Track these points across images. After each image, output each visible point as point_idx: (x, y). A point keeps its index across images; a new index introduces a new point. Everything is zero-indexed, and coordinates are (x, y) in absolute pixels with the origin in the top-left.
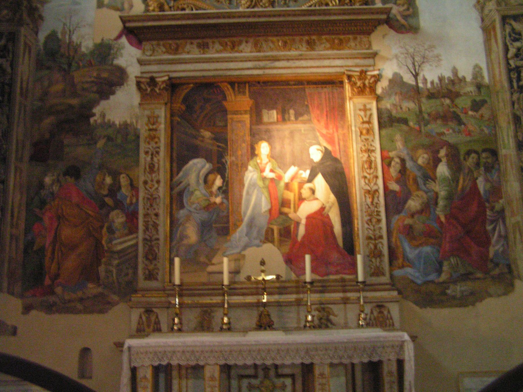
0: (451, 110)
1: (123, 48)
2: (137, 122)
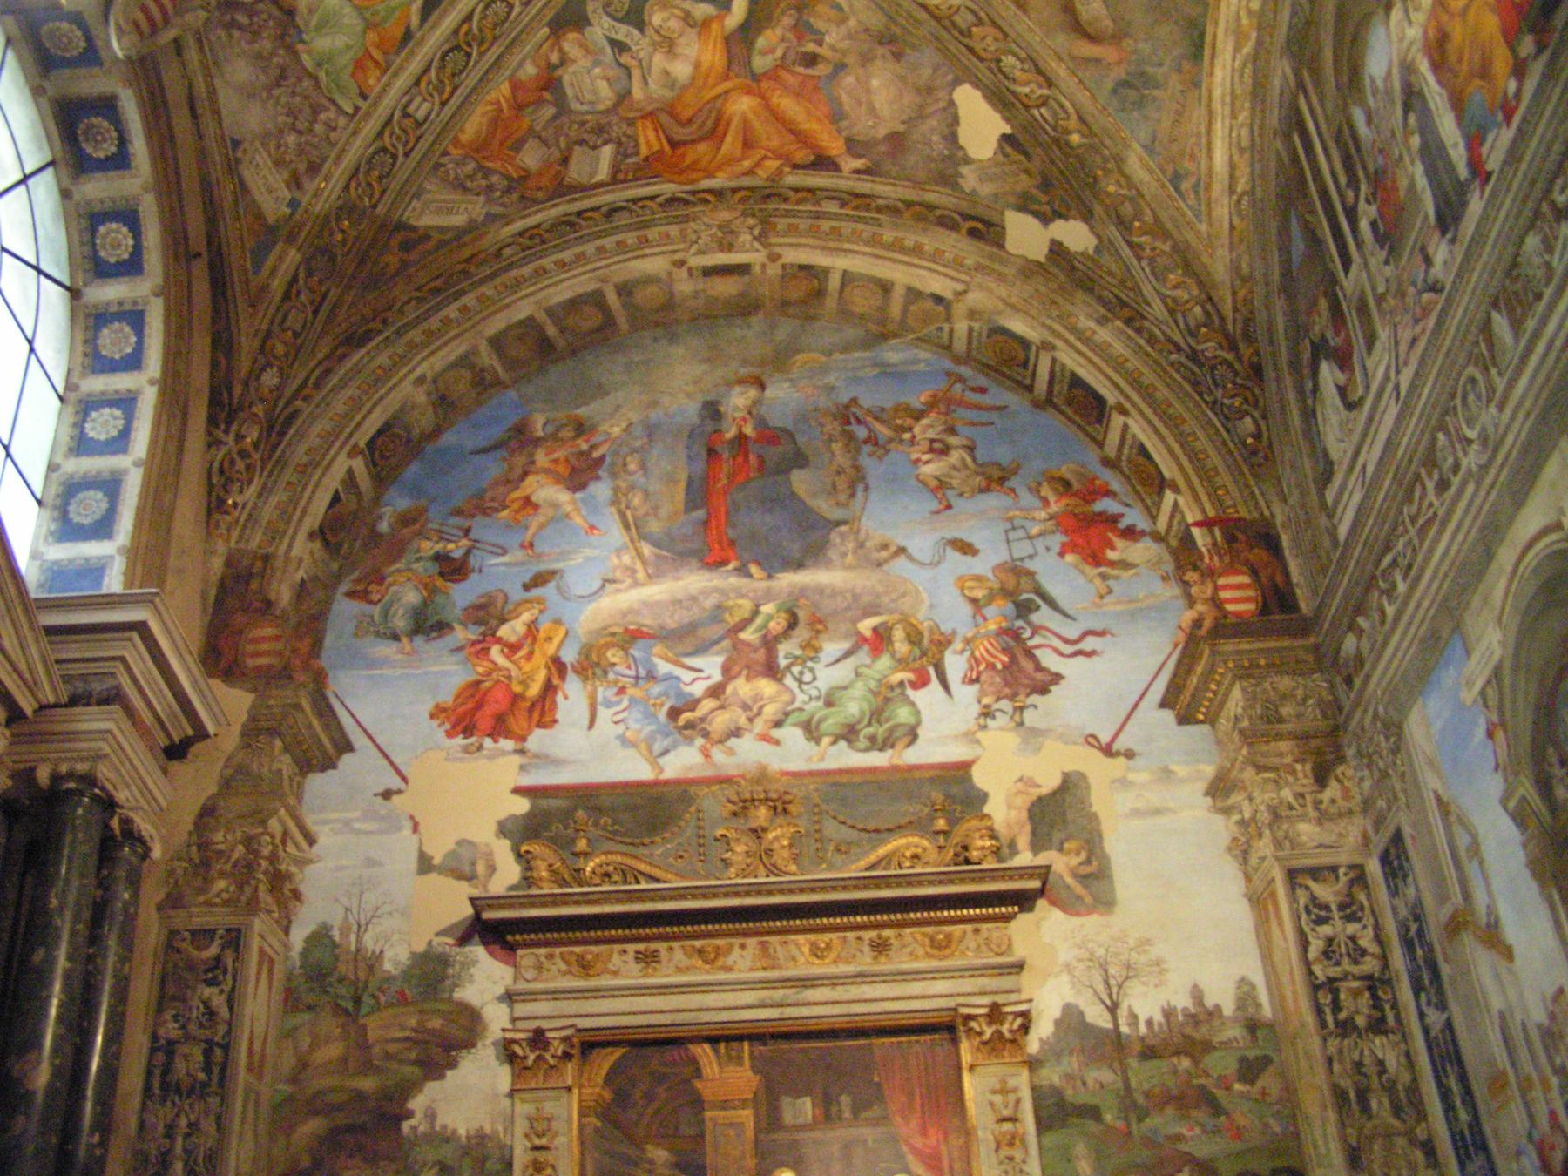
0: (1195, 1082)
1: (474, 962)
2: (505, 1130)
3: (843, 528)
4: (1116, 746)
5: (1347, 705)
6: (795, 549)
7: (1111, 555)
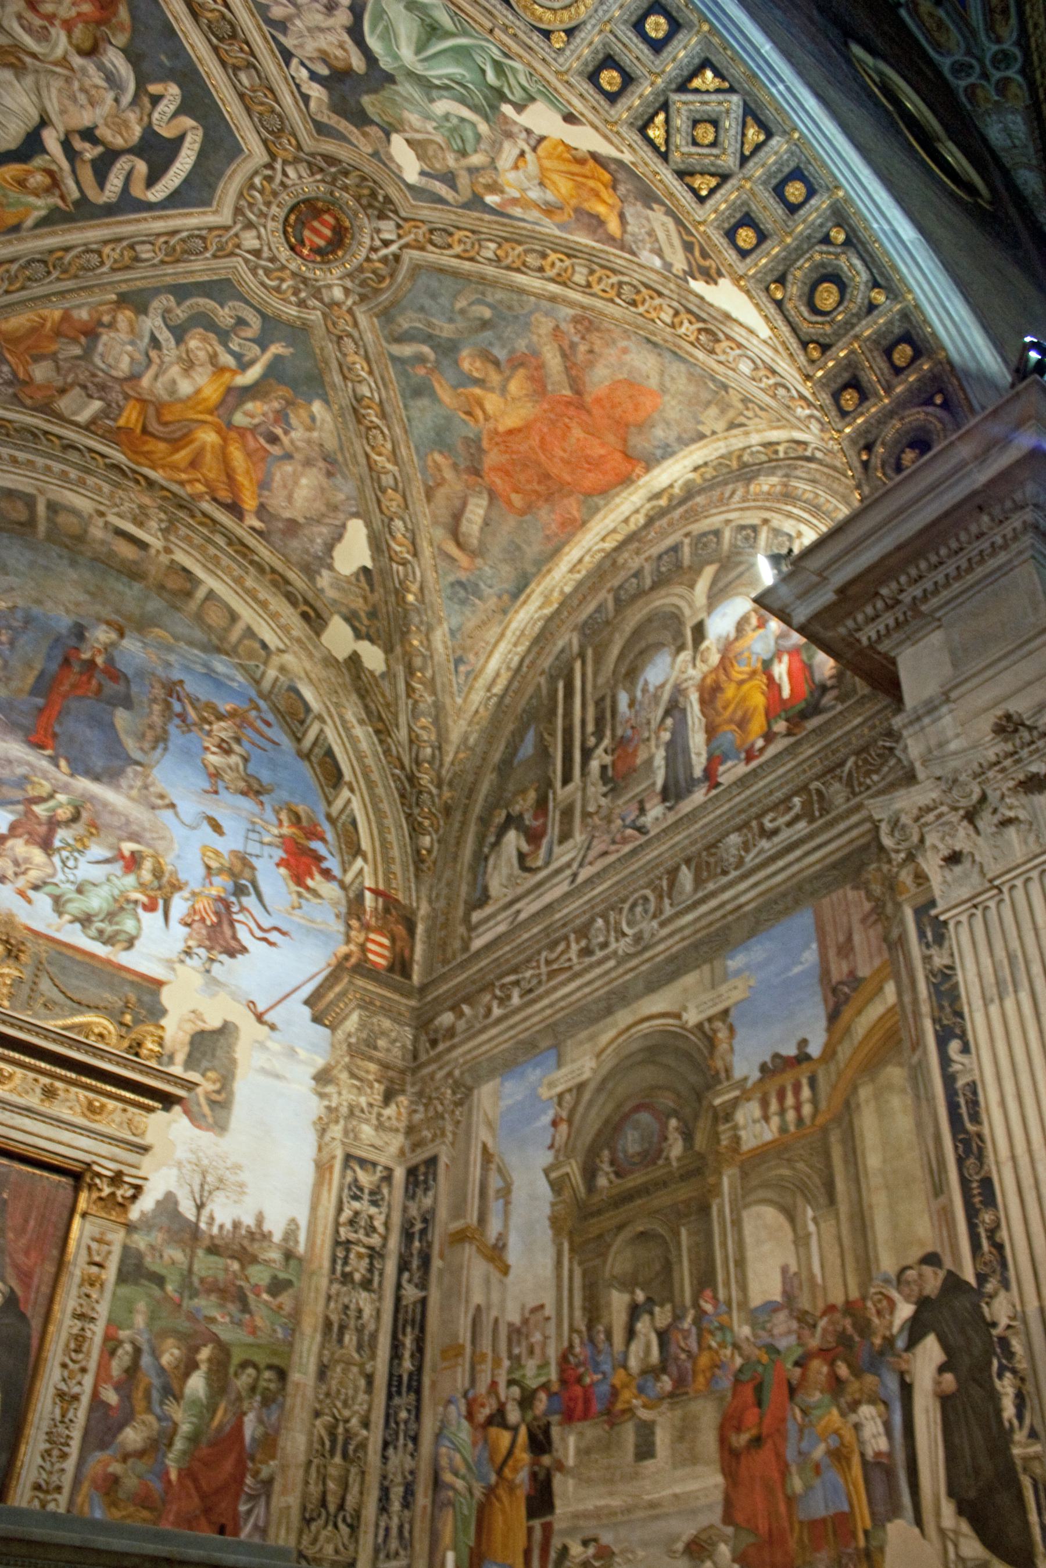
0: (239, 1283)
3: (139, 768)
4: (267, 1018)
5: (423, 1057)
6: (99, 763)
7: (310, 882)
